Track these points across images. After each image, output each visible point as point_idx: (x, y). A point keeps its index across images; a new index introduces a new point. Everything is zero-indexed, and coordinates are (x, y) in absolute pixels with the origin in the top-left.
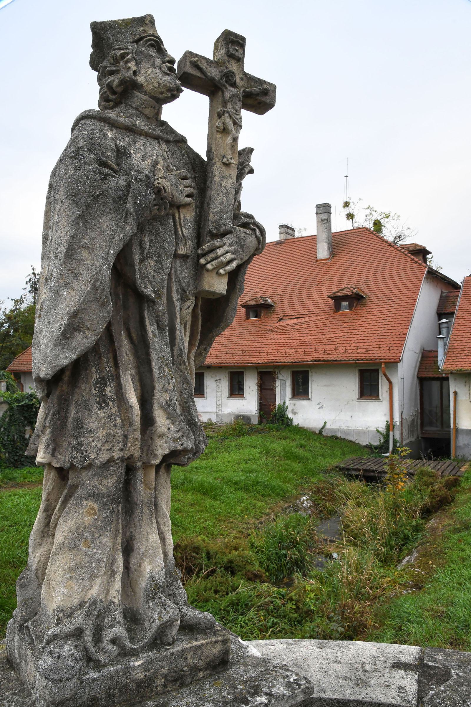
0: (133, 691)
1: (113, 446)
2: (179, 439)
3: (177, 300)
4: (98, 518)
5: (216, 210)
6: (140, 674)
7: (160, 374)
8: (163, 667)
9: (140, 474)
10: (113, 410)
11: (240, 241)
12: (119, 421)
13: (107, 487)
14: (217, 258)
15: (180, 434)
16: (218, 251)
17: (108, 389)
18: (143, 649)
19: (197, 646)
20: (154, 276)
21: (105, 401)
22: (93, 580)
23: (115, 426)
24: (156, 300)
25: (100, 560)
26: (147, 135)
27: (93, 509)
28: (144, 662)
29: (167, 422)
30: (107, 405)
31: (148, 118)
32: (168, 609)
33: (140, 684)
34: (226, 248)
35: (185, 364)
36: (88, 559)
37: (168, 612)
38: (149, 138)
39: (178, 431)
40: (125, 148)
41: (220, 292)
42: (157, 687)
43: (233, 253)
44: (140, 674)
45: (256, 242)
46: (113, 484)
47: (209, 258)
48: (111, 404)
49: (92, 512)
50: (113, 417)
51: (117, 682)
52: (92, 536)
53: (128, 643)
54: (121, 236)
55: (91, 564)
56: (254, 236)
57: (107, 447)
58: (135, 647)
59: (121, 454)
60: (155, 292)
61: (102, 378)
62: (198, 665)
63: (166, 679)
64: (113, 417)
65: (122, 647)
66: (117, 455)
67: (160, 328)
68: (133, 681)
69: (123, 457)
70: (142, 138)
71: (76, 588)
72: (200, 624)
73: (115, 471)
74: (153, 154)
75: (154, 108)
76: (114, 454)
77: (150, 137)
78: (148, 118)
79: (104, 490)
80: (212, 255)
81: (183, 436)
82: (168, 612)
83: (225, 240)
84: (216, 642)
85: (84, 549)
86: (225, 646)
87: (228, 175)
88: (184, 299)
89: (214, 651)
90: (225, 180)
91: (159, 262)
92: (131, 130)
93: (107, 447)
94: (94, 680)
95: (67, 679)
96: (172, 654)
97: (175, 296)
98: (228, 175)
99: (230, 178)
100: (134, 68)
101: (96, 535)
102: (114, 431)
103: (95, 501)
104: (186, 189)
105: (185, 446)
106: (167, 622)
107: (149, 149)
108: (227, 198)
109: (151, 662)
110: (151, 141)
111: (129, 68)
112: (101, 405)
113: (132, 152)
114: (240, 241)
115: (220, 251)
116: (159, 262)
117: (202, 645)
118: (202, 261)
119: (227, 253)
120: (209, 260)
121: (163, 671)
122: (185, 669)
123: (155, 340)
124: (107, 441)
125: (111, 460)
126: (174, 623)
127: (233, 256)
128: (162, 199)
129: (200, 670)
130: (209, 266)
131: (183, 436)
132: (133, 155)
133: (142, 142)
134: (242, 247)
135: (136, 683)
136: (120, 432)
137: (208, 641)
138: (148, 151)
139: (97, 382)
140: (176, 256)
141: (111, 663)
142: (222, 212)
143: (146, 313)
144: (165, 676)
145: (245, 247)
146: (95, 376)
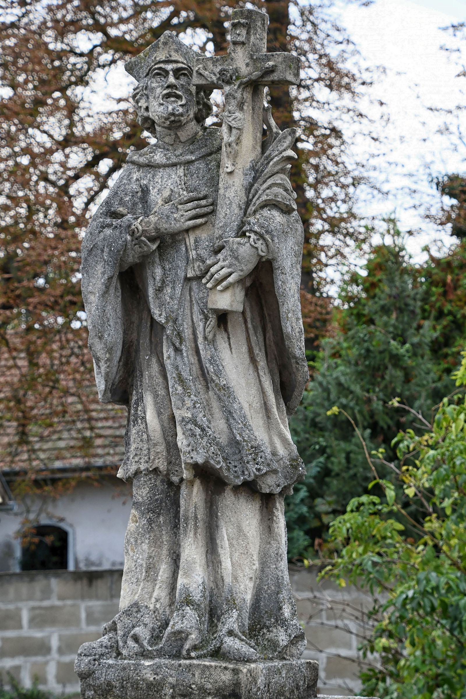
0: (143, 691)
1: (140, 459)
2: (189, 453)
3: (201, 320)
4: (139, 525)
5: (220, 225)
6: (149, 675)
7: (173, 391)
8: (171, 676)
9: (184, 491)
10: (141, 427)
11: (233, 253)
12: (145, 436)
13: (142, 497)
14: (213, 275)
15: (190, 448)
16: (211, 269)
17: (140, 408)
18: (160, 653)
19: (205, 666)
20: (169, 303)
21: (136, 420)
22: (140, 585)
23: (142, 440)
24: (165, 325)
25: (141, 565)
26: (165, 166)
27: (135, 516)
28: (153, 665)
29: (183, 436)
30: (137, 423)
31: (172, 145)
32: (184, 621)
33: (150, 685)
34: (220, 264)
35: (214, 382)
36: (134, 564)
37: (183, 623)
38: (167, 169)
39: (189, 445)
40: (146, 186)
41: (222, 308)
42: (165, 695)
43: (229, 267)
44: (149, 675)
45: (254, 250)
46: (147, 494)
47: (208, 277)
48: (140, 421)
49: (135, 519)
50: (140, 433)
51: (129, 675)
52: (136, 541)
53: (145, 643)
54: (102, 281)
55: (136, 568)
56: (249, 244)
57: (137, 459)
58: (150, 649)
59: (146, 465)
60: (167, 318)
61: (138, 399)
62: (206, 686)
63: (174, 690)
64: (140, 433)
65: (141, 646)
66: (142, 467)
67: (177, 350)
68: (143, 680)
69: (147, 469)
70: (161, 170)
71: (128, 590)
72: (229, 653)
73: (145, 481)
74: (167, 185)
75: (170, 135)
76: (141, 466)
77: (168, 167)
78: (172, 145)
79: (141, 500)
80: (209, 274)
81: (193, 450)
82: (183, 623)
83: (220, 256)
84: (226, 668)
85: (131, 554)
86: (236, 677)
87: (231, 183)
88: (206, 318)
89: (223, 677)
90: (229, 190)
91: (173, 288)
92: (151, 166)
93: (137, 459)
94: (110, 666)
95: (85, 655)
96: (180, 665)
97: (197, 317)
98: (231, 183)
99: (233, 185)
100: (144, 106)
101: (139, 542)
102: (141, 445)
103: (137, 509)
104: (187, 213)
105: (194, 459)
106: (180, 632)
107: (165, 180)
108: (230, 209)
109: (159, 667)
110: (168, 170)
111: (141, 107)
112: (134, 423)
113: (151, 188)
114: (233, 253)
115: (213, 270)
116: (173, 288)
117: (211, 666)
118: (204, 281)
119: (222, 268)
120: (208, 278)
121: (171, 680)
122: (193, 686)
123: (168, 361)
124: (136, 455)
125: (137, 473)
126: (189, 637)
127: (230, 270)
128: (137, 239)
129: (209, 694)
130: (209, 285)
131: (193, 450)
132: (152, 191)
133: (160, 174)
134: (237, 258)
135: (146, 684)
136: (146, 446)
137: (217, 664)
138: (164, 182)
139: (135, 404)
140: (187, 280)
141: (130, 657)
142: (226, 225)
143: (165, 337)
144: (173, 687)
145: (239, 257)
146: (134, 398)
